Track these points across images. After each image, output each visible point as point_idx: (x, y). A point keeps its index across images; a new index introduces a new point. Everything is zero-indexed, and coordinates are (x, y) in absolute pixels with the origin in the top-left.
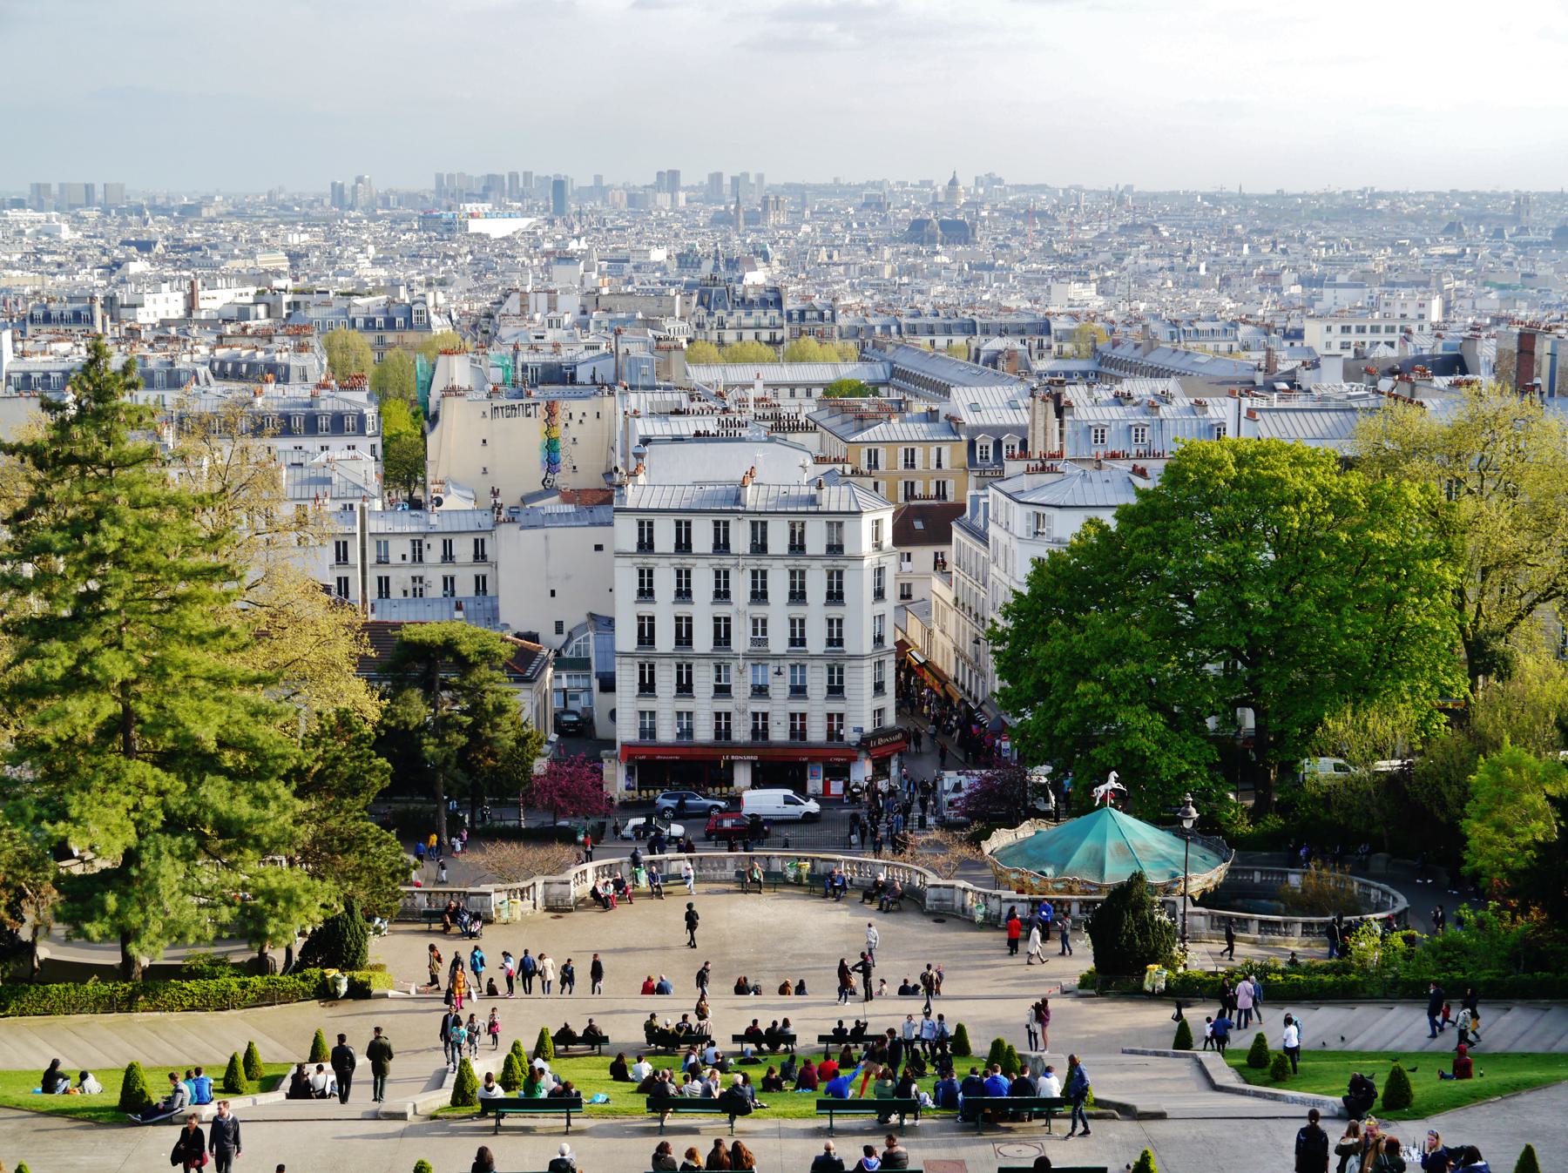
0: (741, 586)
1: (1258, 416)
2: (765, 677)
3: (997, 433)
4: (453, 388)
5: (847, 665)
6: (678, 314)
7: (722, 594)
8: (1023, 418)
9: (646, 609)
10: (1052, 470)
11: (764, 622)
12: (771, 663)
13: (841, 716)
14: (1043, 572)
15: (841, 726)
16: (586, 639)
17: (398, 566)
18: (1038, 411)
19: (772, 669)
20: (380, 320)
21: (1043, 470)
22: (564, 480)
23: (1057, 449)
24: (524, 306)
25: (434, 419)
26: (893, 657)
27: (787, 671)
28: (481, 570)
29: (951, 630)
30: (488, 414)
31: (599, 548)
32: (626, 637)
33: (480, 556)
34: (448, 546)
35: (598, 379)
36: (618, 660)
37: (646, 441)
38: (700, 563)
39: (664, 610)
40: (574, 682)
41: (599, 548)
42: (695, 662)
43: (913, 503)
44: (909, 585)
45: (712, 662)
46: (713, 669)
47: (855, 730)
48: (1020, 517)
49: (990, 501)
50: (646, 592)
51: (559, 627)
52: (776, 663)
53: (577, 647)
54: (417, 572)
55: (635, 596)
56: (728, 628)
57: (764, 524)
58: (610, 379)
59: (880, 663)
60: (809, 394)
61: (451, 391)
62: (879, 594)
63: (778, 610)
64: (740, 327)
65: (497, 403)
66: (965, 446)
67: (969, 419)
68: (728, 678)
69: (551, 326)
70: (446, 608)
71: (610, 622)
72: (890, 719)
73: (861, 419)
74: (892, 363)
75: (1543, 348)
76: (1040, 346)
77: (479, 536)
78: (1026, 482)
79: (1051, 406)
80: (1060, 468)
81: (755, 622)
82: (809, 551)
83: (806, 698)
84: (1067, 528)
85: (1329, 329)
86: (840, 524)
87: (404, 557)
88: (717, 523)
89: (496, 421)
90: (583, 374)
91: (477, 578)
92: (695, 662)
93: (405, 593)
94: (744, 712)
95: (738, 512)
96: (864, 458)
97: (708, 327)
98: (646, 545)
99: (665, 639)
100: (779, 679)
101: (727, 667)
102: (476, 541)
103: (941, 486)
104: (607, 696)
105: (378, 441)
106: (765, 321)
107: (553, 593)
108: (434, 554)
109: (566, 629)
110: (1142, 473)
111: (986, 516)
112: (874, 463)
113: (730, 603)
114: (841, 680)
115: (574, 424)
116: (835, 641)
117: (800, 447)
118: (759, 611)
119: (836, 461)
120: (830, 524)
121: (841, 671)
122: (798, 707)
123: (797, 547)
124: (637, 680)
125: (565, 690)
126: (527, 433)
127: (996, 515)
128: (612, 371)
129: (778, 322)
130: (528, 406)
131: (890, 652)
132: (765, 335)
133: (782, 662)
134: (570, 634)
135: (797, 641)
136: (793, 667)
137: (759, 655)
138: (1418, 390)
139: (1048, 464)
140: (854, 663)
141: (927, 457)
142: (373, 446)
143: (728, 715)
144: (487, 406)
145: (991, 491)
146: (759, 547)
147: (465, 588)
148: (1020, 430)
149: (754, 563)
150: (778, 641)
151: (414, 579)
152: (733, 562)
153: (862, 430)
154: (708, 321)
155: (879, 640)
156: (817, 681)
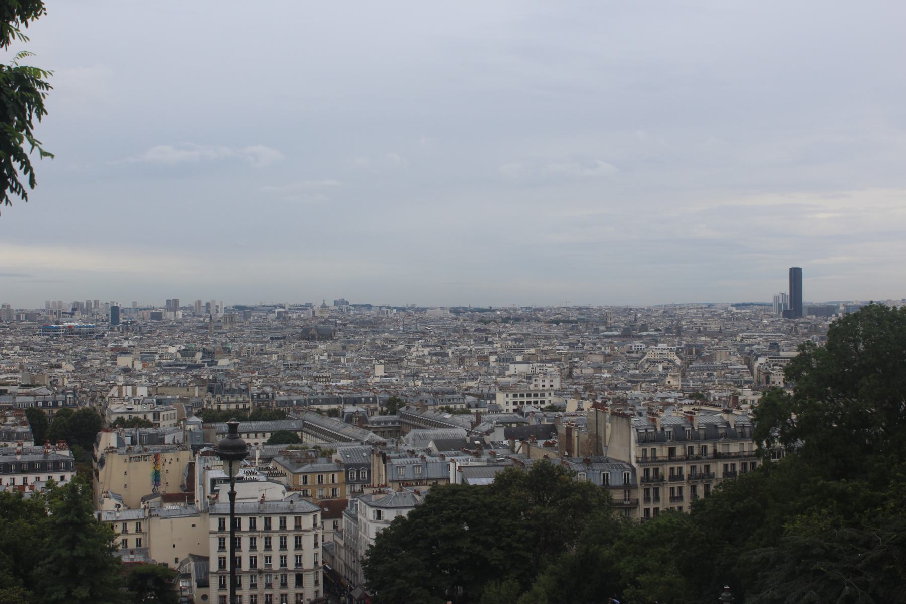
0: (260, 543)
1: (462, 469)
2: (271, 580)
4: (111, 448)
6: (197, 395)
10: (383, 492)
11: (270, 557)
12: (273, 574)
13: (301, 595)
14: (381, 537)
15: (301, 599)
16: (190, 565)
20: (50, 403)
21: (379, 492)
22: (161, 489)
23: (384, 483)
24: (120, 392)
25: (102, 462)
28: (139, 536)
29: (343, 556)
30: (128, 460)
31: (194, 526)
33: (139, 530)
34: (125, 525)
35: (176, 442)
36: (210, 575)
38: (244, 534)
40: (185, 584)
42: (242, 575)
45: (249, 575)
46: (249, 577)
47: (307, 600)
48: (371, 513)
49: (358, 503)
51: (176, 560)
53: (186, 569)
55: (218, 549)
57: (270, 518)
58: (181, 441)
59: (316, 573)
60: (264, 436)
61: (111, 450)
62: (316, 545)
63: (276, 552)
65: (131, 455)
66: (344, 474)
68: (255, 581)
69: (135, 404)
71: (207, 559)
72: (321, 595)
73: (299, 462)
74: (303, 420)
75: (575, 434)
78: (374, 498)
79: (381, 458)
81: (266, 557)
83: (287, 588)
84: (389, 515)
85: (507, 396)
86: (300, 518)
89: (131, 463)
90: (168, 439)
91: (137, 539)
92: (242, 575)
94: (262, 594)
95: (260, 514)
96: (301, 480)
97: (213, 403)
100: (277, 581)
102: (137, 523)
103: (334, 490)
105: (75, 473)
106: (241, 399)
107: (174, 546)
109: (180, 561)
110: (418, 493)
112: (305, 482)
113: (257, 551)
115: (167, 464)
116: (299, 564)
117: (279, 482)
118: (268, 553)
120: (296, 518)
122: (284, 591)
123: (283, 526)
126: (145, 468)
127: (361, 510)
129: (247, 399)
130: (146, 456)
131: (321, 568)
132: (241, 406)
133: (277, 574)
134: (181, 563)
135: (284, 564)
137: (268, 572)
138: (531, 448)
139: (382, 489)
141: (328, 479)
143: (256, 596)
145: (359, 501)
146: (268, 527)
147: (132, 545)
149: (266, 534)
150: (276, 565)
152: (257, 534)
153: (299, 467)
154: (213, 400)
155: (316, 563)
156: (292, 580)
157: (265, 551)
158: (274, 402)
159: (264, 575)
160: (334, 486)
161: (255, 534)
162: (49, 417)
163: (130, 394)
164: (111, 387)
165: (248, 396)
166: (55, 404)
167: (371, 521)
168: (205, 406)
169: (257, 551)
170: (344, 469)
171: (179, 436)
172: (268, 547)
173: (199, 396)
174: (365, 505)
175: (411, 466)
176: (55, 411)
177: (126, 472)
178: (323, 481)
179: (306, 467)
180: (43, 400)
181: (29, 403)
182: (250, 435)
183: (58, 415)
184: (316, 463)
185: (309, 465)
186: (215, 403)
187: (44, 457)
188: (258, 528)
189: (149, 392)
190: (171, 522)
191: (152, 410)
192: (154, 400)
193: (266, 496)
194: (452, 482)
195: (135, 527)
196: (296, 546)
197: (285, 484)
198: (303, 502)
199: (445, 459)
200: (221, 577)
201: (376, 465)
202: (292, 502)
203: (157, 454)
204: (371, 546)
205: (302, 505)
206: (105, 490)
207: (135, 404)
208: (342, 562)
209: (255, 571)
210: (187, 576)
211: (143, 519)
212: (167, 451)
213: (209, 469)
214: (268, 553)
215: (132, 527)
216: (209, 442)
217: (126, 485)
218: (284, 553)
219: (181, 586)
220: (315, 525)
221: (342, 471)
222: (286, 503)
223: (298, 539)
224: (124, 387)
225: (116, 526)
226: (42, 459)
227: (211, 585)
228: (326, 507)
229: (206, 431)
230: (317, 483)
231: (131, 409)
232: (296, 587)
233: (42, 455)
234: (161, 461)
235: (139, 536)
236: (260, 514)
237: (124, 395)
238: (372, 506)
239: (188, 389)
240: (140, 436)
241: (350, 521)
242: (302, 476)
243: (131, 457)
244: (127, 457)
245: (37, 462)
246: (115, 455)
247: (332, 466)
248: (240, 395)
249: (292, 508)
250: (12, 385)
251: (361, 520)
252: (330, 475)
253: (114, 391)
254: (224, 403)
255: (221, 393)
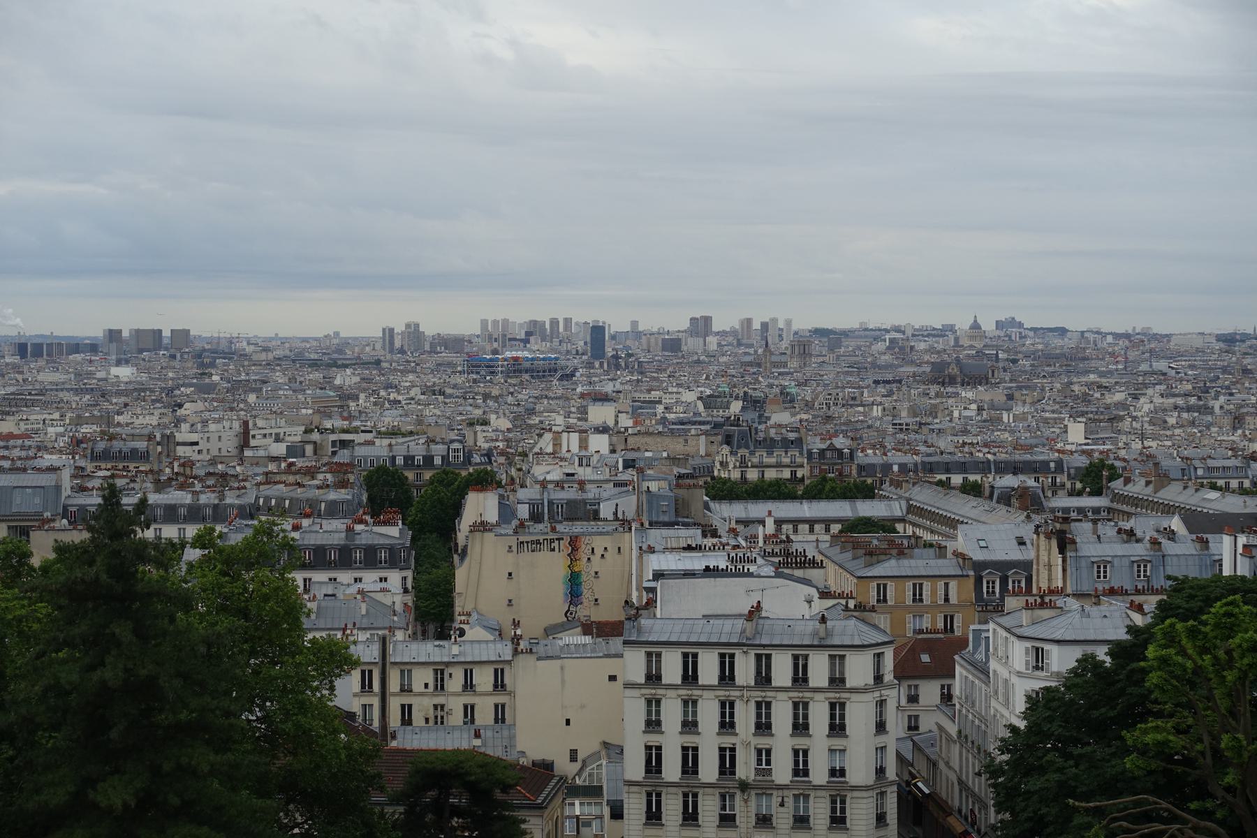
0: (745, 717)
2: (769, 807)
3: (1003, 567)
4: (482, 523)
5: (849, 795)
6: (702, 452)
7: (727, 725)
8: (1028, 554)
9: (654, 739)
10: (1051, 606)
11: (769, 752)
12: (775, 793)
14: (1039, 703)
17: (421, 694)
18: (1042, 548)
19: (775, 800)
20: (419, 459)
21: (1042, 605)
22: (585, 611)
24: (557, 444)
25: (464, 554)
26: (895, 788)
27: (790, 802)
28: (500, 699)
30: (514, 548)
31: (613, 678)
32: (635, 768)
33: (499, 685)
34: (468, 675)
35: (620, 517)
37: (658, 575)
38: (706, 694)
39: (672, 743)
40: (586, 809)
41: (613, 678)
42: (701, 791)
43: (920, 637)
44: (917, 717)
45: (717, 791)
46: (717, 797)
48: (1019, 654)
49: (991, 634)
50: (653, 724)
51: (573, 755)
52: (780, 793)
53: (590, 775)
54: (439, 700)
56: (733, 758)
57: (769, 657)
59: (882, 794)
60: (827, 530)
61: (482, 527)
62: (881, 727)
63: (782, 742)
64: (761, 466)
65: (522, 539)
66: (971, 583)
67: (978, 556)
68: (732, 808)
69: (580, 465)
70: (465, 735)
73: (870, 554)
74: (908, 500)
76: (1054, 483)
77: (499, 666)
78: (1025, 617)
79: (1054, 543)
80: (1060, 603)
81: (759, 752)
82: (812, 684)
84: (1062, 661)
86: (842, 657)
87: (426, 686)
88: (722, 656)
90: (606, 511)
91: (496, 706)
93: (427, 720)
95: (744, 645)
96: (873, 593)
97: (731, 466)
98: (653, 678)
99: (672, 769)
100: (781, 809)
101: (732, 796)
102: (496, 671)
103: (949, 620)
104: (617, 823)
105: (409, 574)
106: (786, 460)
107: (568, 722)
108: (455, 682)
109: (580, 756)
110: (1139, 608)
111: (987, 650)
114: (843, 810)
115: (596, 559)
117: (806, 582)
118: (763, 742)
119: (840, 596)
120: (832, 657)
121: (843, 802)
123: (800, 678)
124: (645, 809)
125: (577, 817)
127: (996, 649)
128: (634, 507)
129: (799, 460)
130: (552, 541)
131: (892, 783)
133: (786, 793)
134: (584, 761)
135: (800, 770)
136: (796, 797)
137: (764, 787)
139: (1047, 599)
140: (856, 794)
141: (934, 592)
142: (405, 579)
144: (513, 541)
146: (764, 679)
147: (485, 716)
148: (1026, 566)
149: (758, 695)
150: (782, 771)
151: (436, 707)
152: (738, 693)
155: (880, 771)
157: (754, 735)
158: (854, 467)
159: (753, 792)
160: (949, 611)
161: (732, 693)
162: (415, 486)
163: (575, 448)
164: (540, 436)
165: (801, 454)
166: (428, 460)
167: (1019, 674)
168: (716, 473)
169: (737, 735)
170: (971, 573)
171: (629, 504)
172: (763, 727)
173: (706, 455)
174: (1005, 634)
175: (1126, 562)
176: (427, 475)
177: (510, 574)
178: (924, 597)
179: (889, 567)
180: (406, 454)
181: (378, 458)
182: (800, 527)
183: (431, 482)
184: (912, 557)
185: (893, 562)
186: (735, 467)
187: (347, 537)
188: (740, 680)
189: (610, 445)
190: (562, 668)
191: (612, 478)
192: (621, 461)
193: (763, 605)
194: (1227, 571)
195: (491, 679)
196: (832, 727)
197: (821, 586)
198: (853, 622)
199: (1207, 548)
200: (649, 795)
201: (1044, 557)
202: (823, 620)
203: (576, 537)
204: (1013, 729)
205: (847, 629)
206: (468, 608)
207: (580, 465)
208: (953, 777)
209: (730, 784)
210: (593, 792)
211: (509, 662)
212: (601, 534)
213: (651, 550)
214: (763, 742)
215: (484, 679)
216: (688, 517)
217: (510, 601)
218: (801, 742)
219: (578, 813)
220: (878, 678)
221: (967, 576)
222: (812, 623)
223: (837, 709)
224: (565, 435)
225: (451, 675)
226: (342, 543)
227: (625, 811)
228: (924, 652)
229: (681, 492)
230: (909, 601)
231: (573, 475)
232: (830, 828)
233: (343, 535)
234: (583, 553)
235: (500, 699)
236: (744, 645)
237: (564, 448)
238: (1020, 637)
239: (686, 441)
240: (551, 503)
241: (970, 677)
242: (875, 584)
243: (522, 543)
244: (513, 541)
245: (332, 547)
246: (489, 536)
247: (947, 566)
248: (786, 452)
249: (822, 634)
250: (363, 431)
251: (995, 671)
252: (941, 584)
253: (546, 443)
254: (752, 467)
255: (747, 448)
